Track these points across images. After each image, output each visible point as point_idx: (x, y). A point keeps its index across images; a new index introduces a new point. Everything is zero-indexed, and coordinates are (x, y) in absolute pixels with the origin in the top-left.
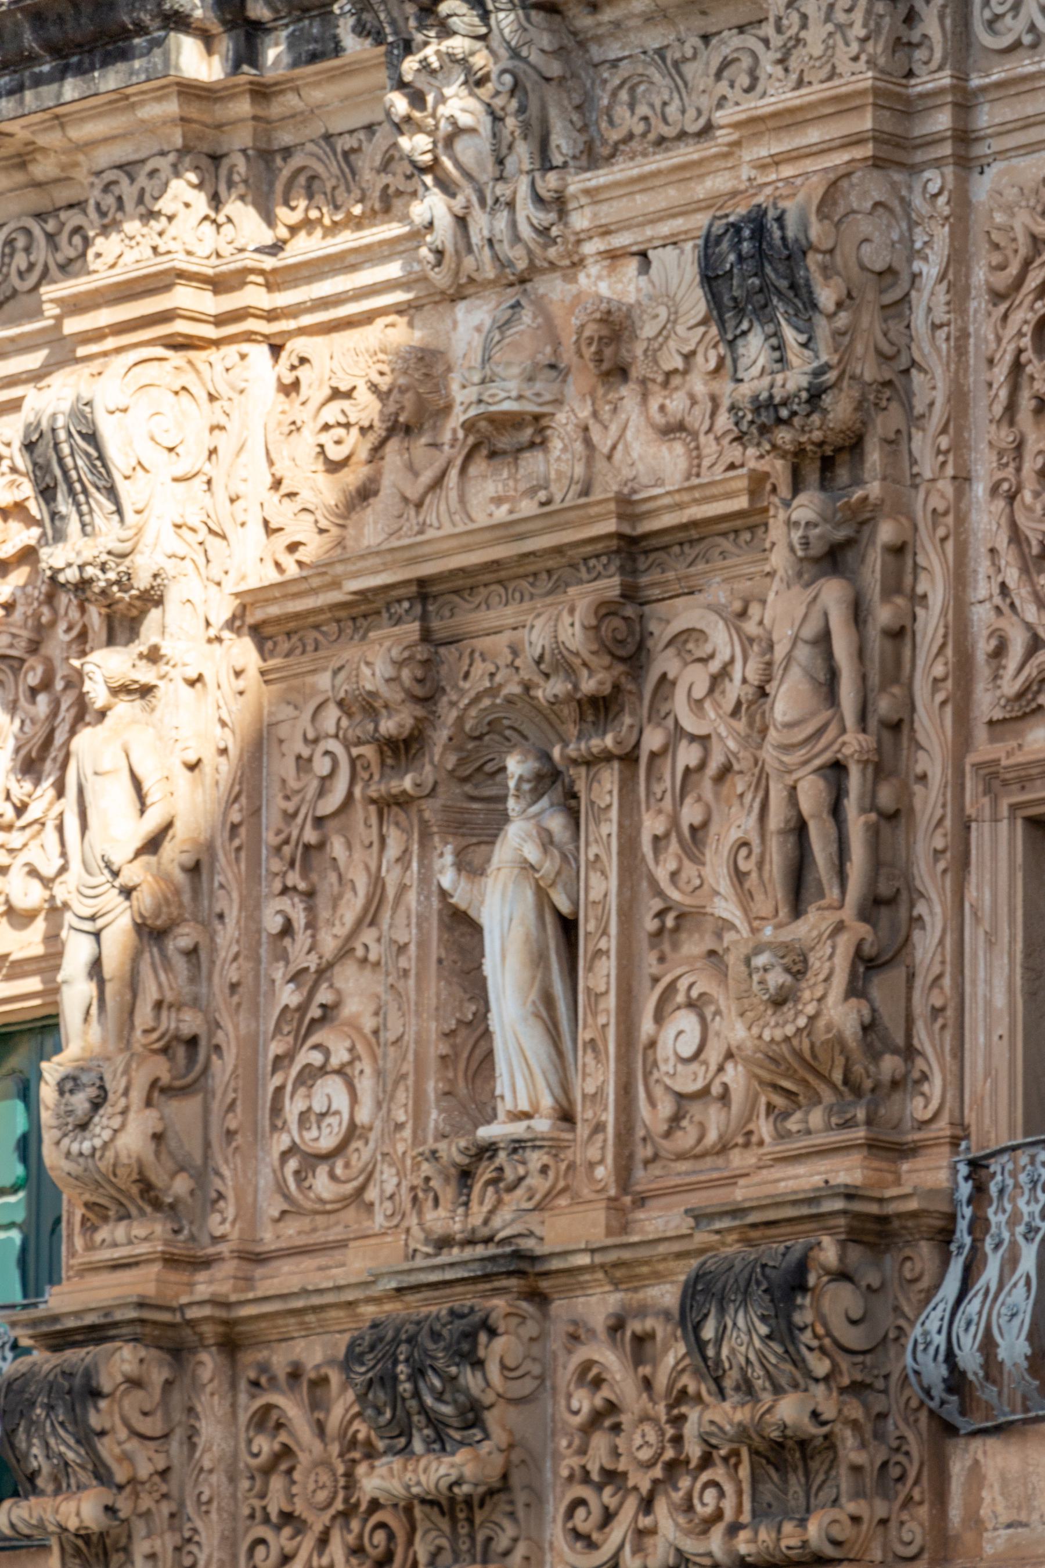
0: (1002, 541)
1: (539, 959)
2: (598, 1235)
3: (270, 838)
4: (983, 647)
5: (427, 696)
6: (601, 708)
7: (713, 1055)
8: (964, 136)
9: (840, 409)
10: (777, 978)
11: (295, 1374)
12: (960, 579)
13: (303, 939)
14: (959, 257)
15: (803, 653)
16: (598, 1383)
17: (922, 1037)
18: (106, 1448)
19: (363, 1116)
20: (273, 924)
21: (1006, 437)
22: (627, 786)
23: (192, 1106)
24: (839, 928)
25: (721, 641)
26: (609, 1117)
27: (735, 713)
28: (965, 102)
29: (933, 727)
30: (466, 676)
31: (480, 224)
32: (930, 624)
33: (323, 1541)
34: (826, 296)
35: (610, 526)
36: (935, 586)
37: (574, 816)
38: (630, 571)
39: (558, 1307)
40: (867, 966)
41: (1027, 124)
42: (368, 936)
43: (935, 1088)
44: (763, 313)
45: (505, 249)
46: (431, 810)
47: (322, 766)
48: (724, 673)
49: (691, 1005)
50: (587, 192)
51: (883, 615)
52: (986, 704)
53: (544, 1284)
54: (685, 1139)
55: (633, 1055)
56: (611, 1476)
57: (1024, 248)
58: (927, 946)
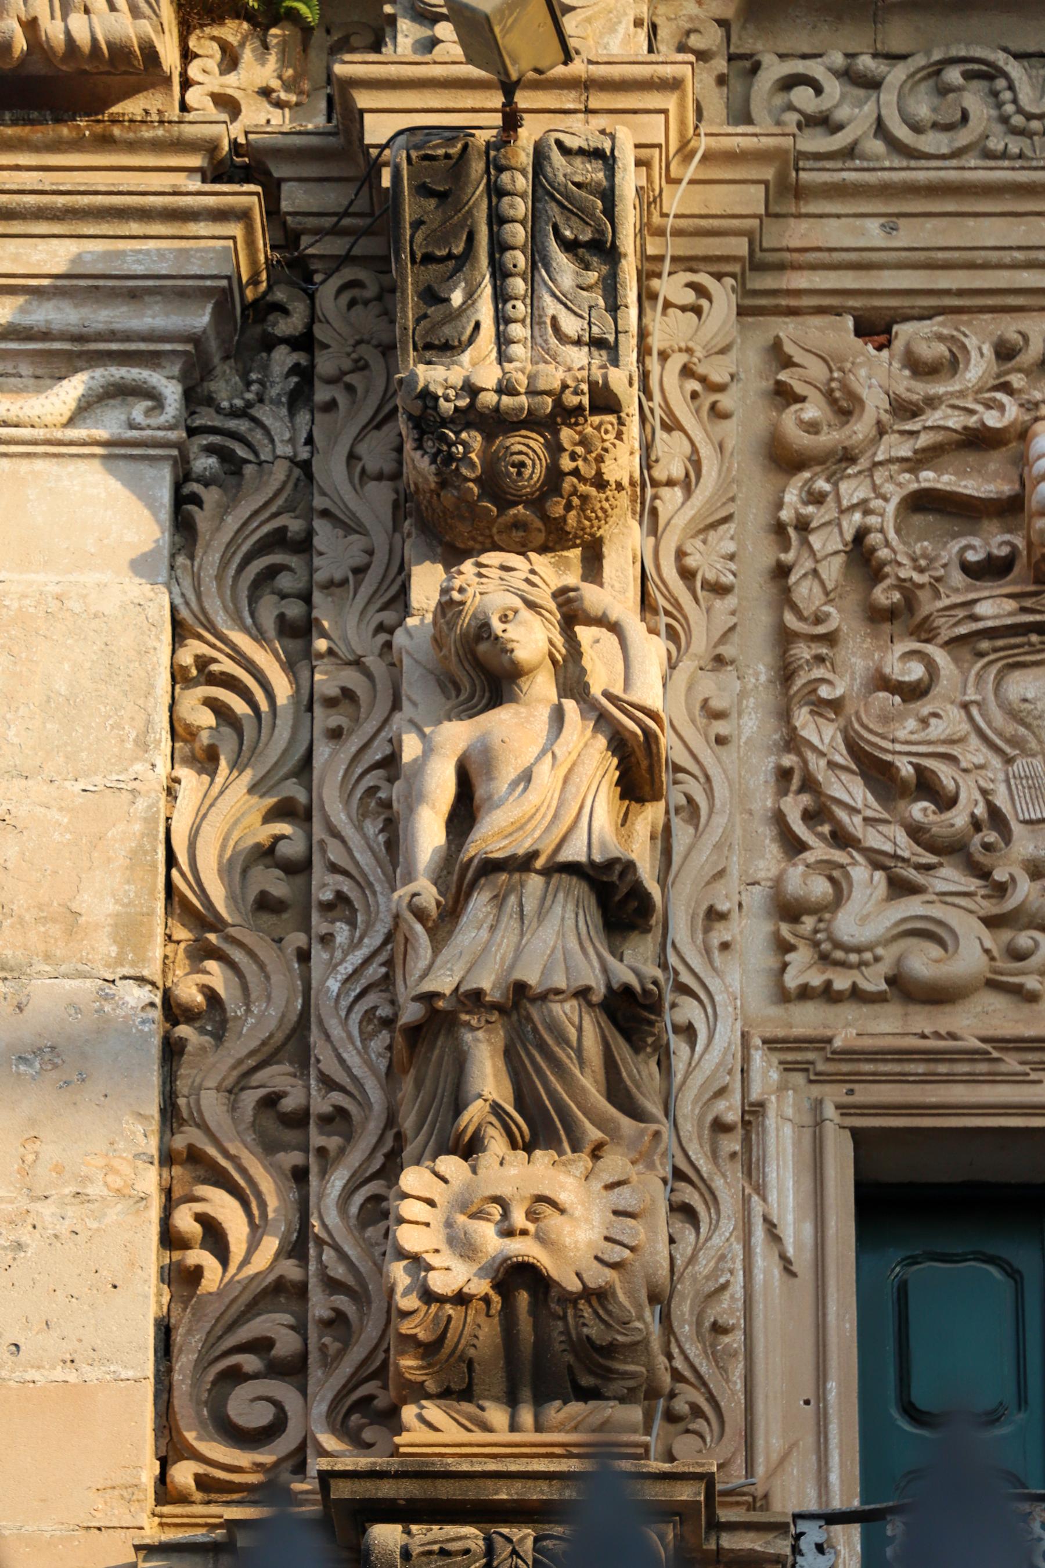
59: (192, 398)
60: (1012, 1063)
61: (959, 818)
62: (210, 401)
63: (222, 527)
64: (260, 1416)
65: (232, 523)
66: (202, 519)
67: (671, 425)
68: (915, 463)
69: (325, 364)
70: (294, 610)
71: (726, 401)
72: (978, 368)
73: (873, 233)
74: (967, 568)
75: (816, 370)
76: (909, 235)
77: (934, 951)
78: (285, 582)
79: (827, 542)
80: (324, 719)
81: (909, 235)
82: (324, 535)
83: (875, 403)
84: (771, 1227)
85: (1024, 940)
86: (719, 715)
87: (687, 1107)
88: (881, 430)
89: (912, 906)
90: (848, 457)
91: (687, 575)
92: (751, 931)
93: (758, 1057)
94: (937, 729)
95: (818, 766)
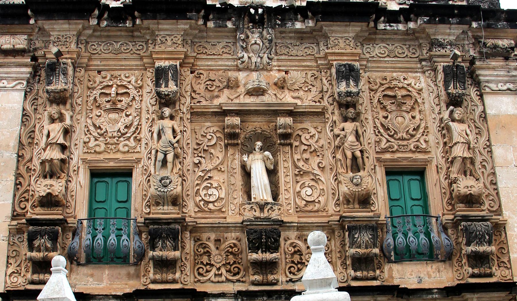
7: (316, 195)
19: (223, 196)
30: (248, 128)
31: (254, 59)
41: (378, 67)
44: (347, 79)
50: (278, 59)
57: (379, 85)
59: (28, 82)
60: (106, 161)
61: (102, 132)
62: (30, 82)
63: (29, 98)
64: (24, 206)
65: (30, 97)
66: (27, 96)
67: (76, 86)
68: (101, 89)
69: (41, 79)
70: (36, 107)
71: (82, 83)
72: (108, 78)
73: (99, 63)
74: (106, 102)
75: (92, 77)
76: (103, 63)
77: (99, 148)
78: (35, 104)
79: (92, 98)
80: (37, 121)
81: (103, 63)
82: (39, 99)
83: (98, 82)
84: (80, 182)
85: (108, 146)
86: (79, 120)
87: (71, 168)
88: (98, 85)
89: (97, 142)
90: (95, 88)
91: (76, 103)
92: (82, 144)
93: (80, 161)
94: (101, 121)
95: (89, 125)
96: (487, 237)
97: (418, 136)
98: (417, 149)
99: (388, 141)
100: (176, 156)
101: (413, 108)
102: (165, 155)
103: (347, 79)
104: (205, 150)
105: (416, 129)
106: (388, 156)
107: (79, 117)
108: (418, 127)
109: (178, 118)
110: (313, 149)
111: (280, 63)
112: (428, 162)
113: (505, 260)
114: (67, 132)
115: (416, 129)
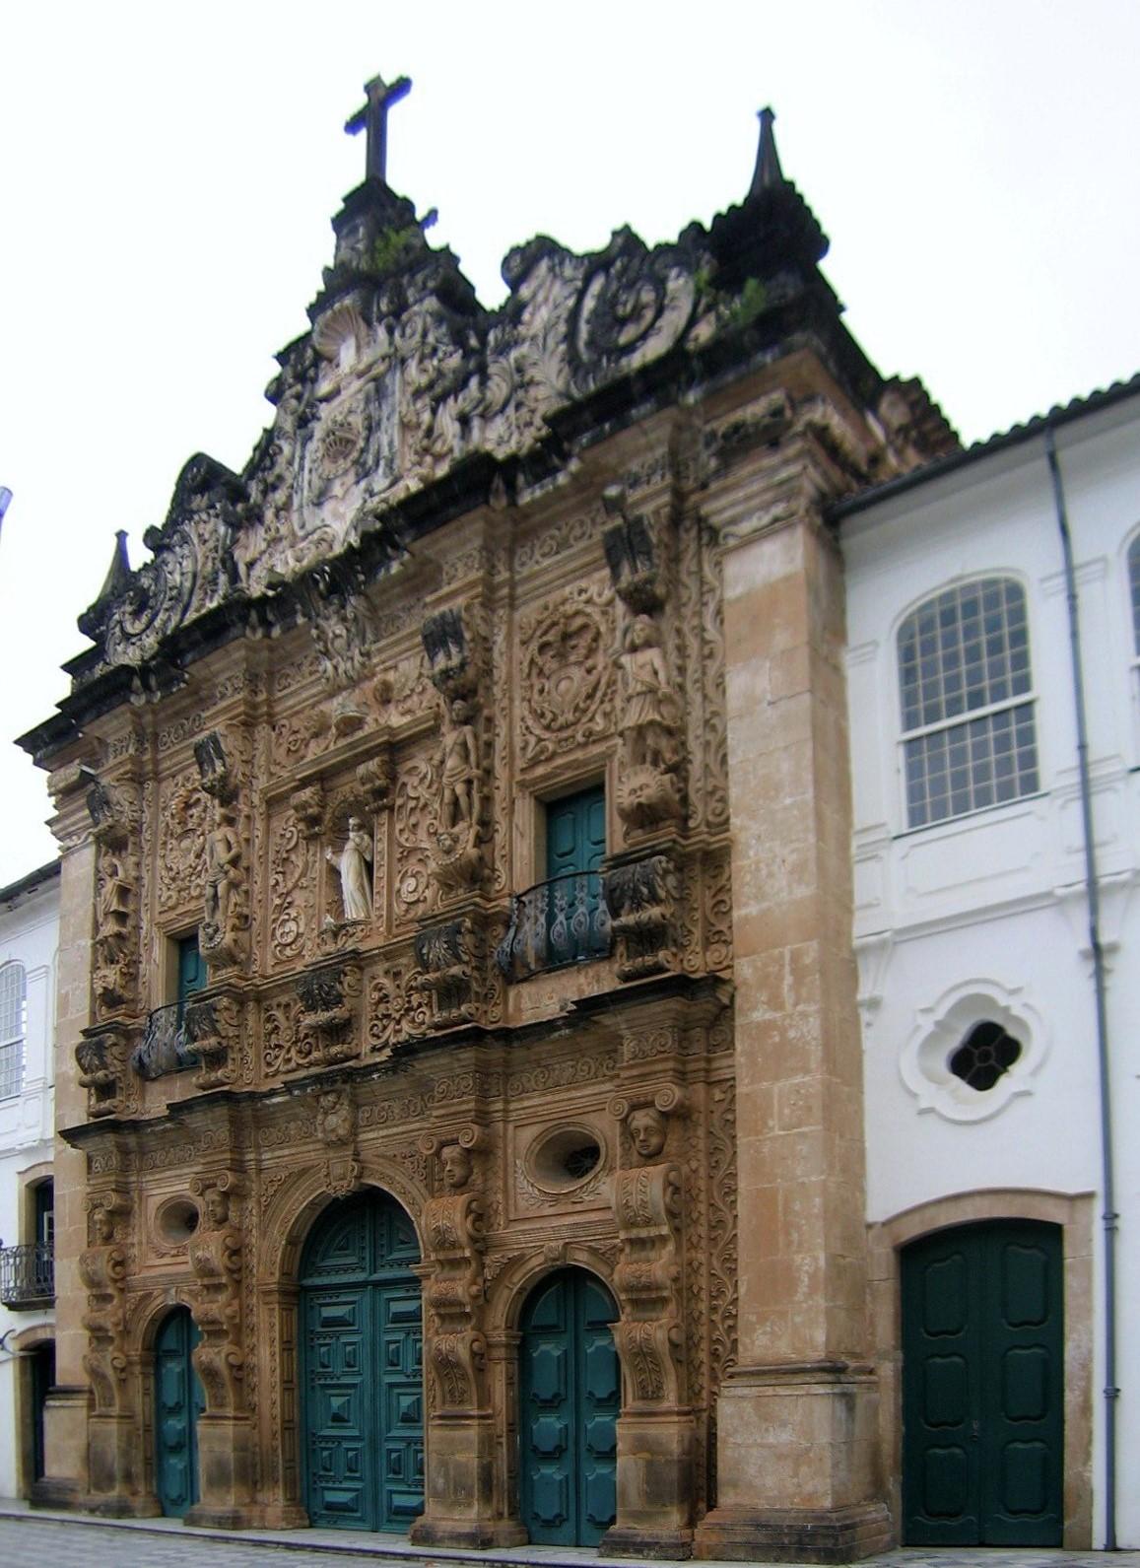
0: (526, 713)
1: (360, 875)
2: (381, 944)
3: (271, 857)
4: (518, 742)
5: (323, 805)
6: (380, 793)
8: (512, 597)
9: (471, 672)
10: (448, 842)
11: (279, 1005)
12: (511, 729)
13: (282, 884)
14: (509, 636)
15: (457, 748)
16: (380, 990)
17: (498, 865)
18: (218, 1026)
20: (272, 882)
21: (526, 683)
22: (391, 818)
23: (246, 935)
24: (470, 826)
25: (424, 767)
26: (384, 913)
27: (429, 787)
28: (512, 584)
29: (501, 772)
32: (499, 743)
33: (288, 1051)
34: (467, 635)
35: (385, 738)
36: (502, 729)
37: (372, 836)
38: (392, 754)
39: (367, 970)
40: (480, 841)
42: (303, 880)
43: (503, 879)
45: (351, 673)
46: (324, 839)
47: (288, 835)
48: (425, 777)
49: (413, 876)
51: (485, 737)
52: (520, 763)
53: (363, 963)
54: (409, 916)
55: (393, 894)
56: (387, 1016)
58: (499, 838)
96: (645, 890)
97: (593, 708)
98: (591, 738)
99: (540, 740)
100: (233, 885)
101: (591, 652)
102: (216, 887)
103: (444, 644)
104: (286, 860)
105: (590, 696)
106: (540, 771)
107: (149, 860)
108: (595, 688)
109: (242, 820)
110: (422, 801)
111: (384, 656)
112: (608, 756)
113: (723, 927)
114: (123, 892)
115: (590, 696)
